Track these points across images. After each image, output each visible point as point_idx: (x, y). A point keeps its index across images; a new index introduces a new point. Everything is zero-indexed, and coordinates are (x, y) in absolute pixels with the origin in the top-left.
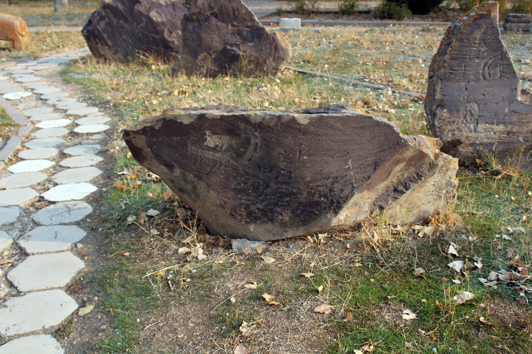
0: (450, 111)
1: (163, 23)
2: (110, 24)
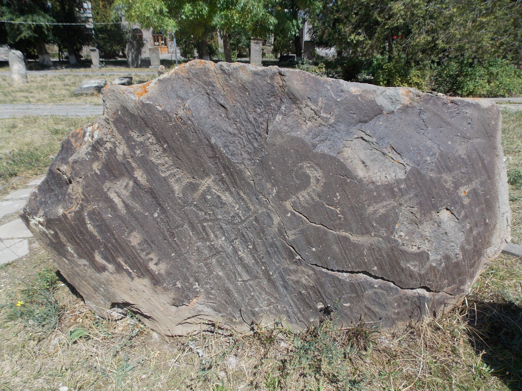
1: (391, 190)
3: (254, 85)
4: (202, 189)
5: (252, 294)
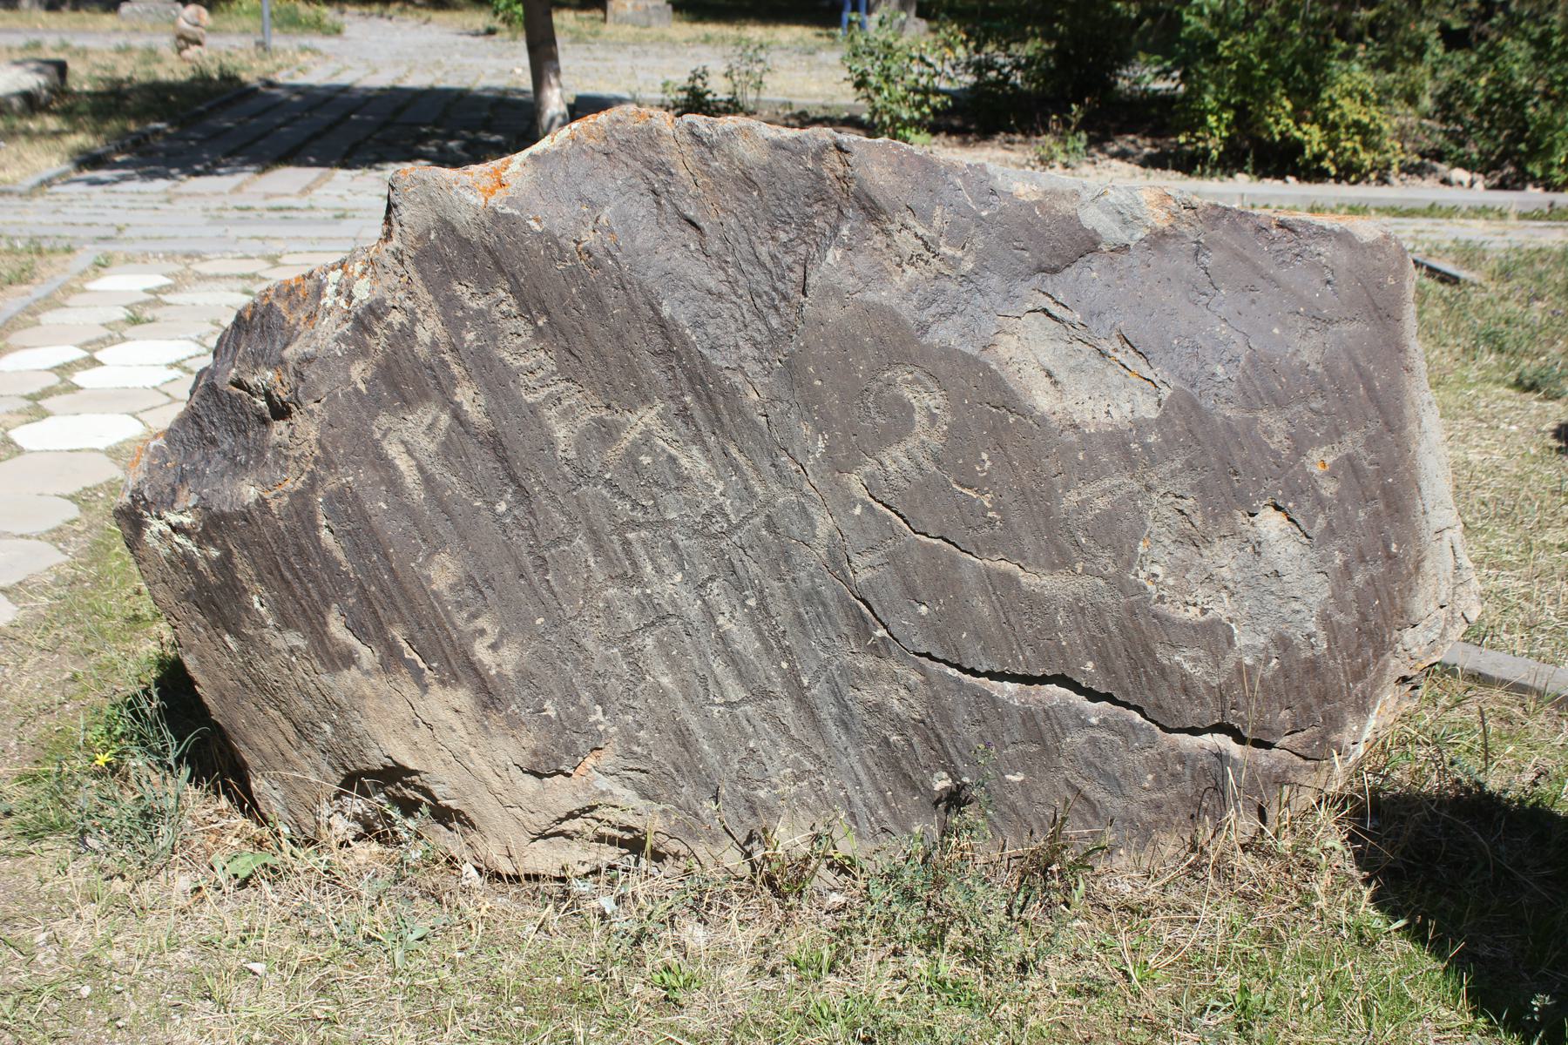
1: (1121, 446)
3: (774, 174)
4: (630, 436)
5: (752, 745)
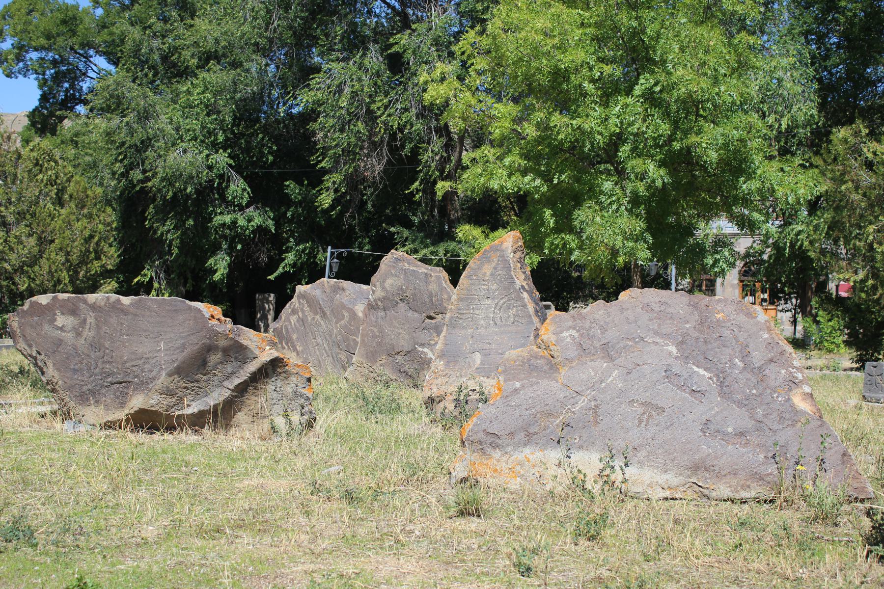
0: (447, 364)
2: (302, 321)
